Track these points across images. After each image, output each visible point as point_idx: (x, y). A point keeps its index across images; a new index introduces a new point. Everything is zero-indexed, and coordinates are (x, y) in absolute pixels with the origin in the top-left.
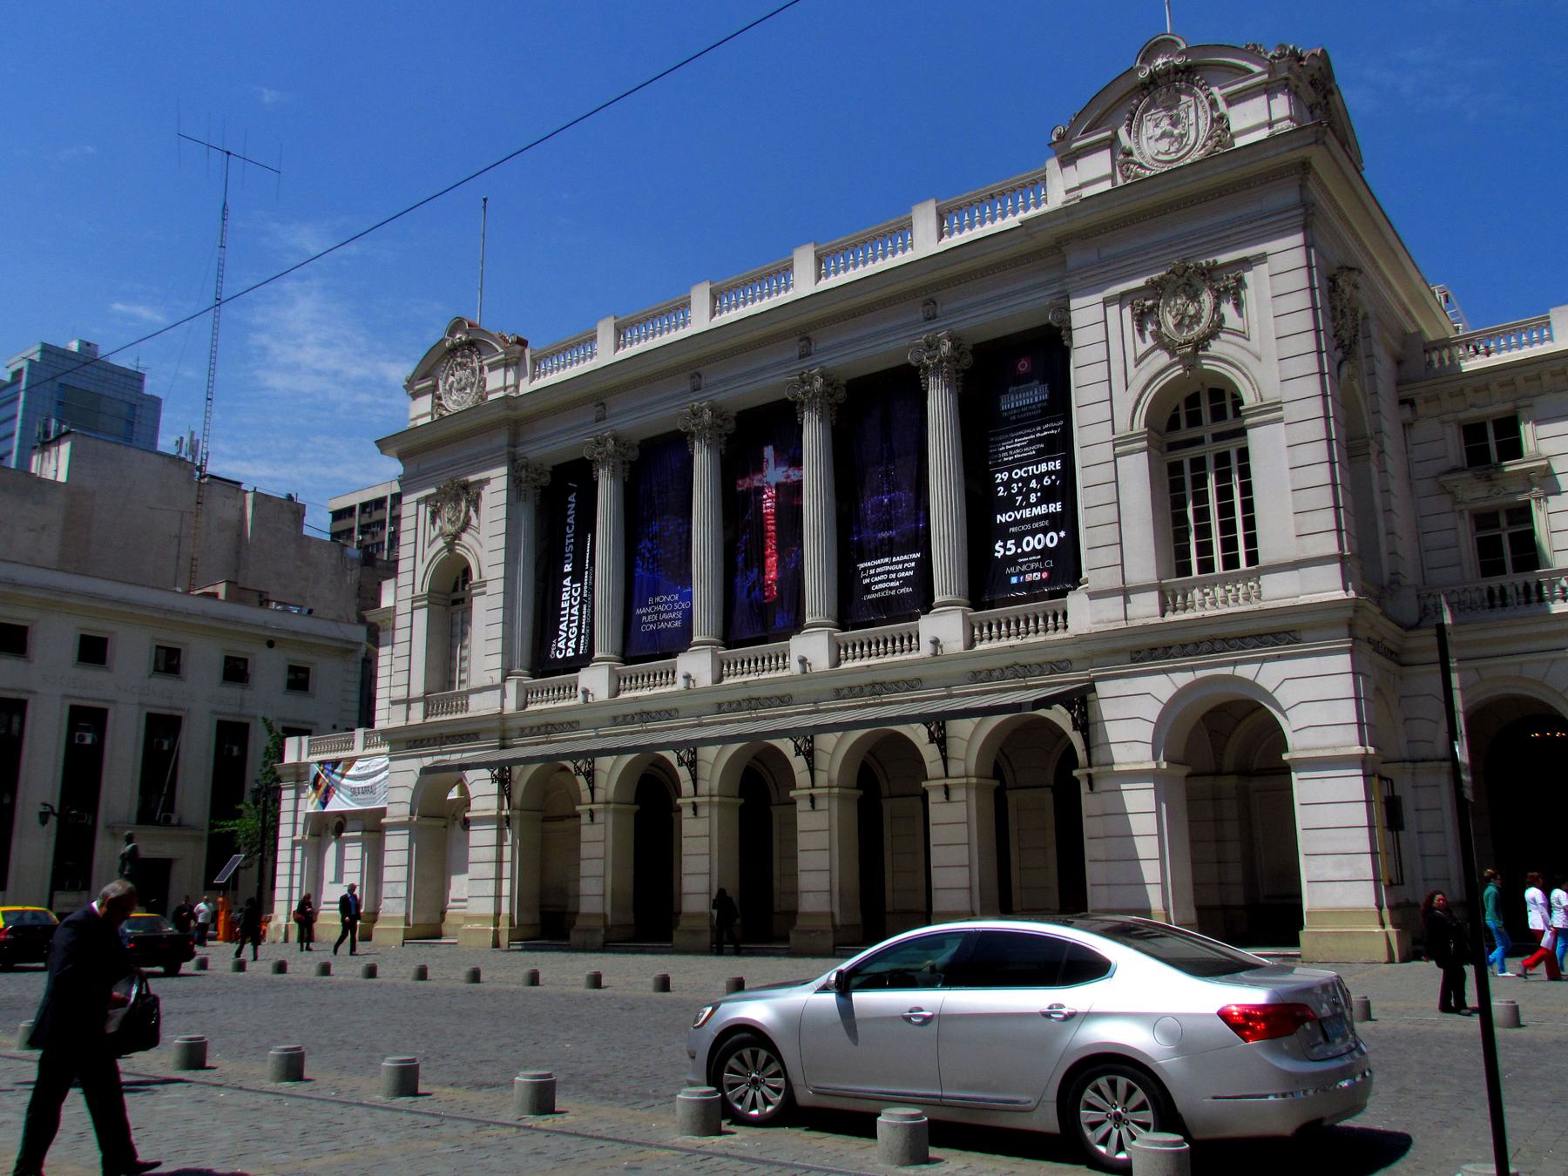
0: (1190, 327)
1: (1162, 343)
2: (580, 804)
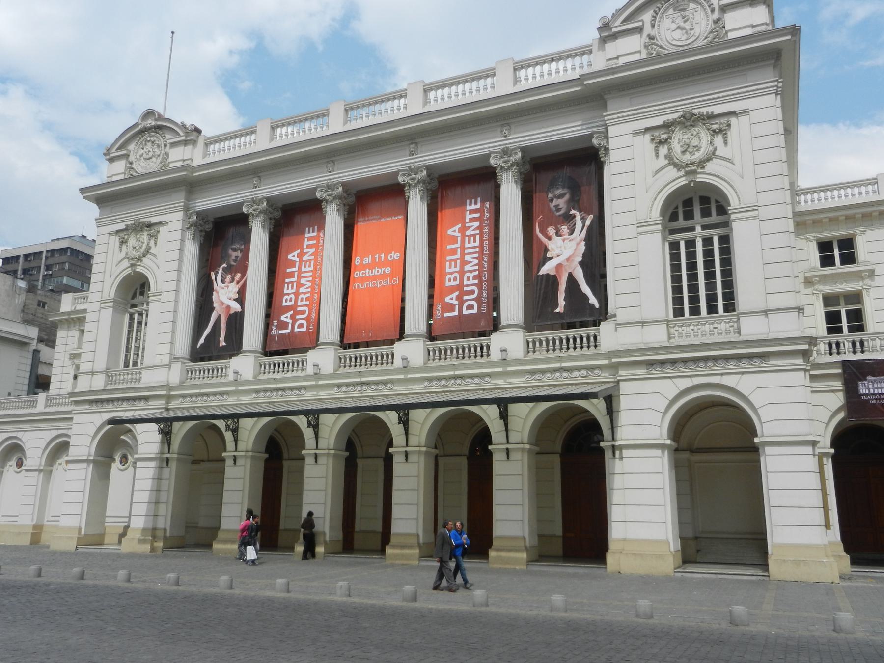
2: (225, 451)
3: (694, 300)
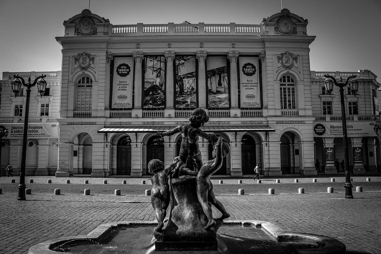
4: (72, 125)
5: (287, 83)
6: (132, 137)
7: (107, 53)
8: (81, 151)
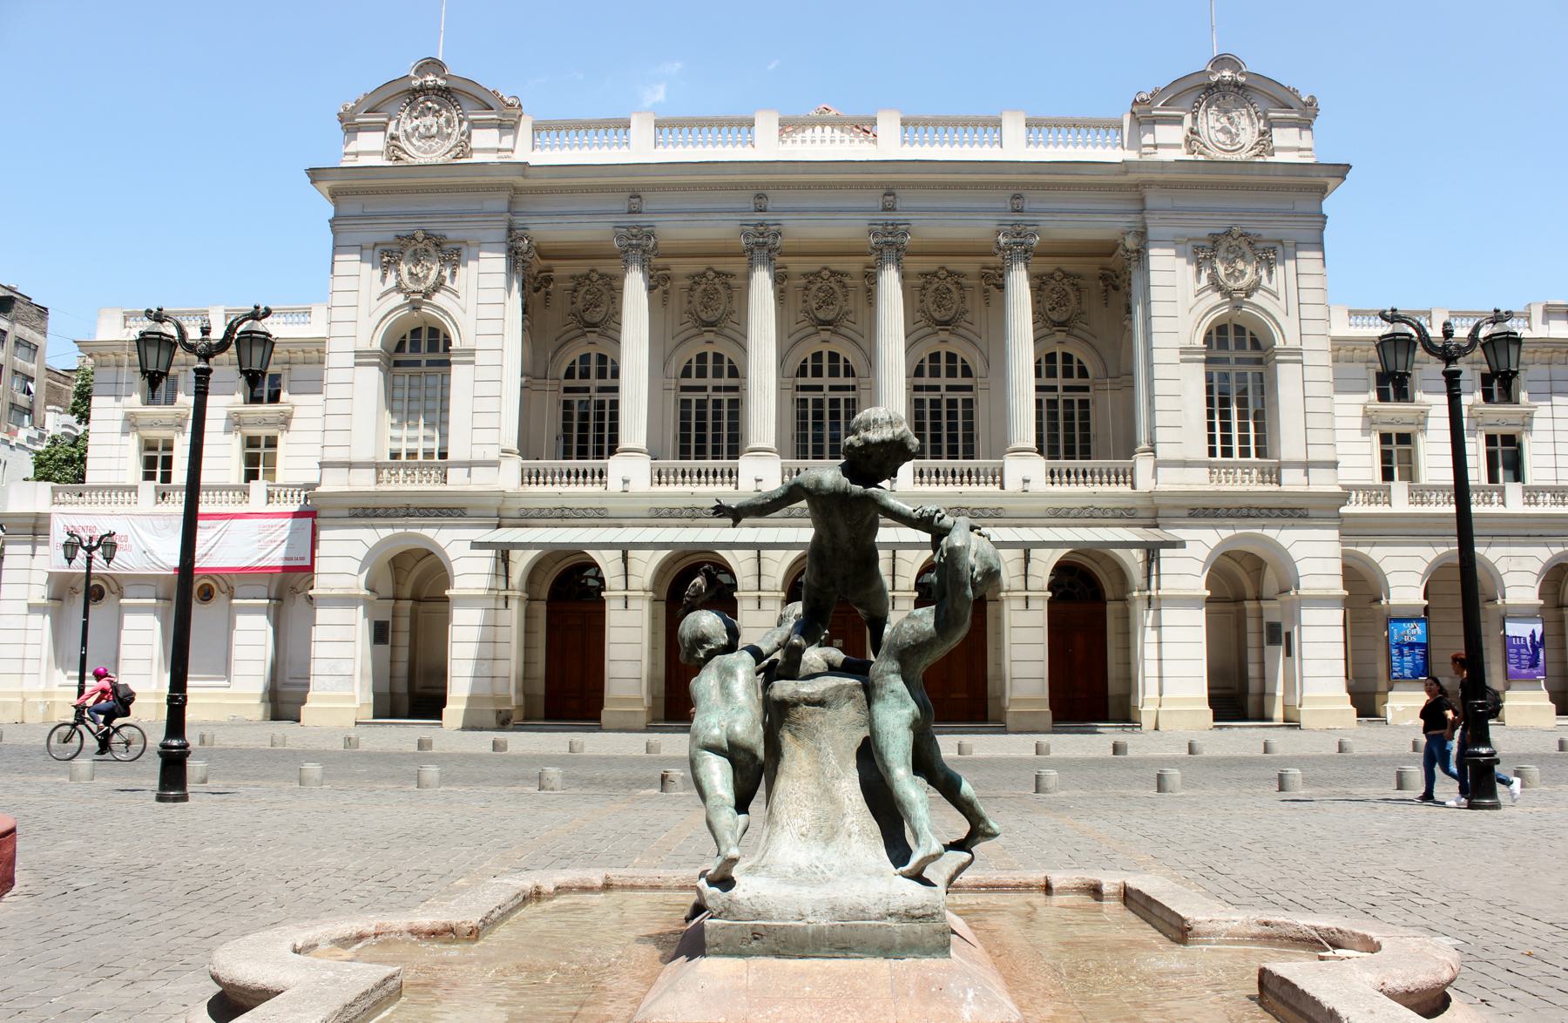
0: (1237, 279)
1: (1215, 285)
3: (1226, 439)
4: (367, 516)
5: (1232, 353)
6: (609, 563)
7: (510, 230)
8: (404, 624)
